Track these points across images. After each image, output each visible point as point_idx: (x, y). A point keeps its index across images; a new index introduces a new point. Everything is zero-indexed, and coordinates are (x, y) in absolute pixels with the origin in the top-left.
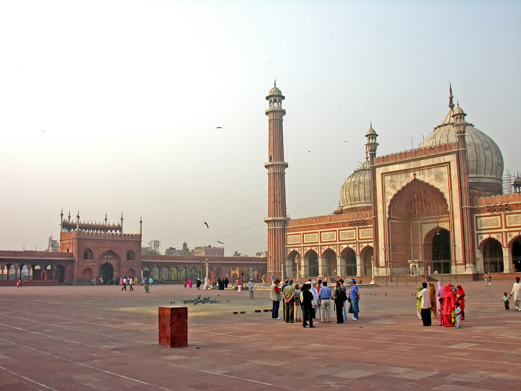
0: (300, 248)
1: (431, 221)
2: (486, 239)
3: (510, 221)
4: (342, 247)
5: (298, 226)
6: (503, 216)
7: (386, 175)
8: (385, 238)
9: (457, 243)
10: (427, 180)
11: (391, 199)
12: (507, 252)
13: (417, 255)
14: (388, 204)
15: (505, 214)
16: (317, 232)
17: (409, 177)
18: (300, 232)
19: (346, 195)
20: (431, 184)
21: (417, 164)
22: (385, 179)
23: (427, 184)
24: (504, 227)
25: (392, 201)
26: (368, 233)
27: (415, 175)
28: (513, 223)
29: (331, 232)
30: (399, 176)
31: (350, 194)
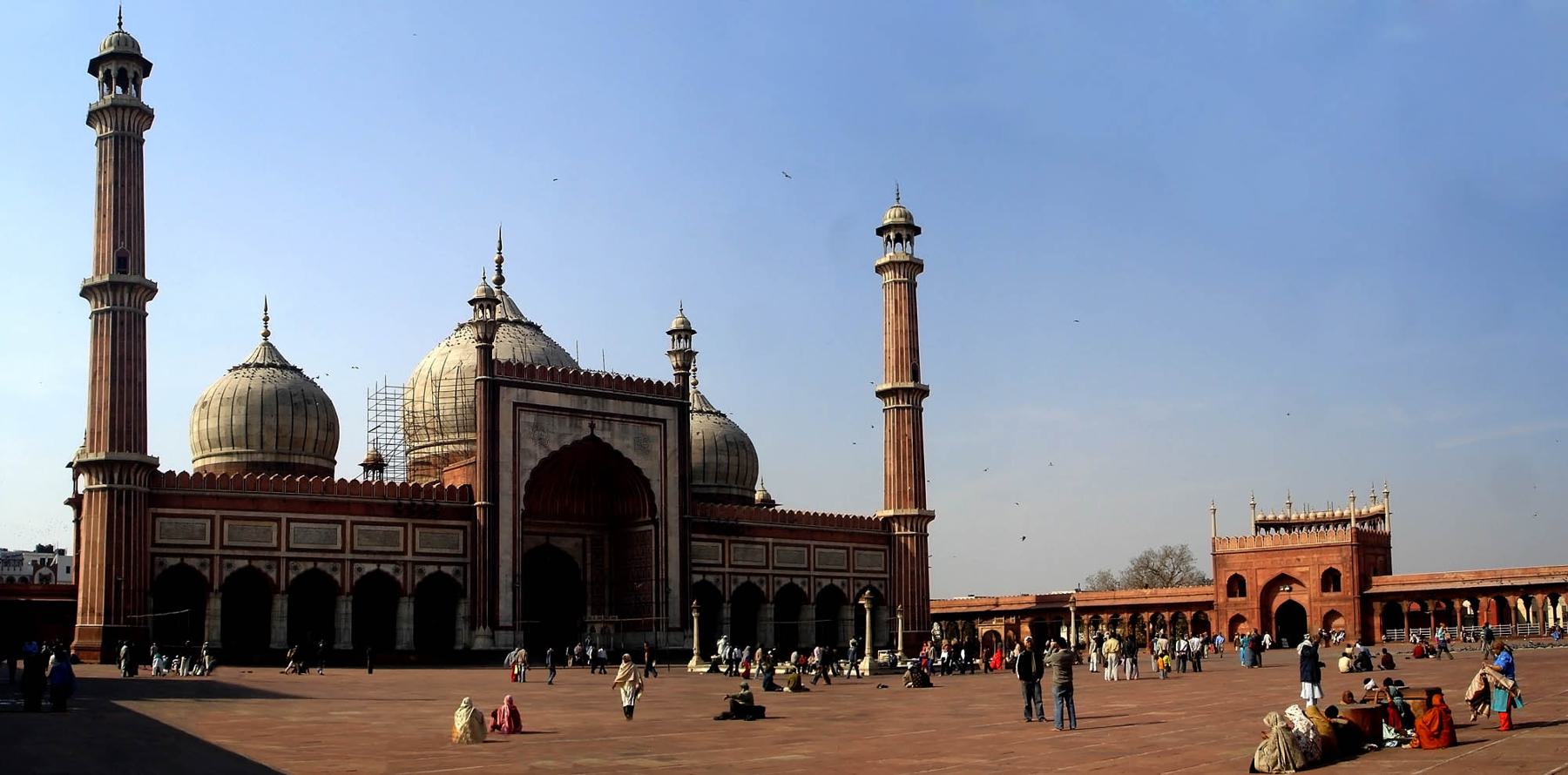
0: (208, 560)
1: (533, 530)
4: (360, 570)
5: (208, 494)
6: (727, 543)
9: (671, 586)
10: (617, 445)
12: (729, 612)
14: (525, 478)
15: (731, 542)
16: (278, 520)
18: (212, 512)
20: (626, 456)
23: (618, 454)
24: (727, 565)
25: (535, 472)
27: (592, 426)
29: (325, 526)
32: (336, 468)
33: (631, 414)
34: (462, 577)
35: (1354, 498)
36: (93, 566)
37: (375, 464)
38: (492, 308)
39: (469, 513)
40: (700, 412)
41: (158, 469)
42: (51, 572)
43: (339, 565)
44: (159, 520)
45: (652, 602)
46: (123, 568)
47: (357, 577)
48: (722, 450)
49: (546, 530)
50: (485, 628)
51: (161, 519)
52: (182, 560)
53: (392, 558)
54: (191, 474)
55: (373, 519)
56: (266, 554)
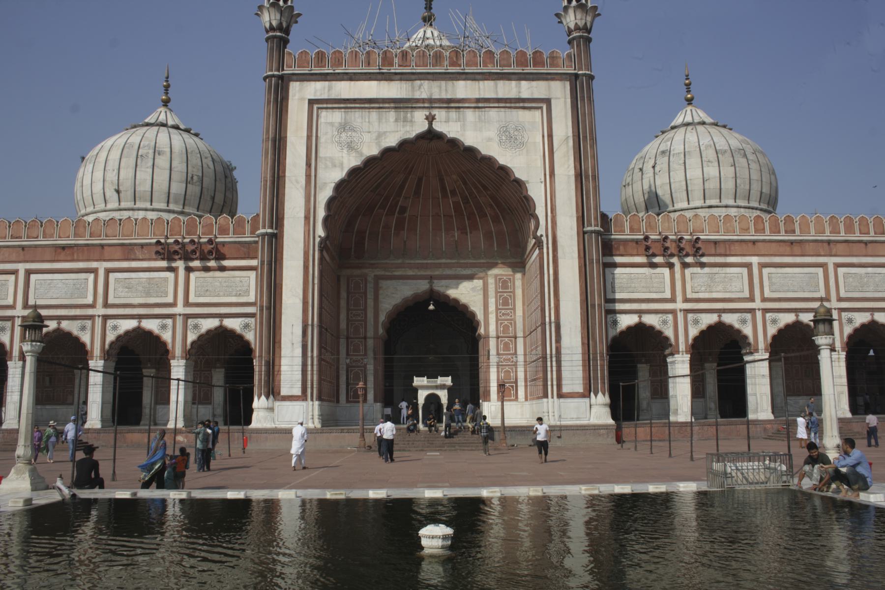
1: (410, 273)
2: (630, 329)
3: (696, 285)
4: (115, 328)
6: (678, 267)
7: (325, 106)
8: (307, 303)
10: (469, 139)
13: (358, 367)
14: (325, 194)
15: (685, 265)
17: (408, 124)
19: (104, 181)
21: (440, 90)
22: (322, 120)
23: (471, 152)
24: (679, 298)
25: (340, 186)
26: (224, 285)
27: (431, 119)
28: (703, 289)
30: (374, 114)
31: (120, 178)
34: (252, 333)
43: (89, 323)
47: (111, 337)
48: (709, 161)
49: (429, 273)
50: (259, 398)
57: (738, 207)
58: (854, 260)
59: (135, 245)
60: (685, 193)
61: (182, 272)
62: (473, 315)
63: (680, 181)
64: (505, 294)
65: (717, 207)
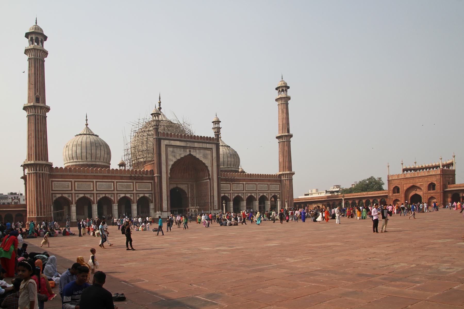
0: (71, 195)
2: (223, 196)
4: (119, 196)
5: (69, 174)
9: (215, 197)
10: (198, 156)
11: (172, 164)
14: (170, 167)
15: (232, 184)
16: (93, 182)
18: (71, 180)
20: (200, 159)
22: (168, 150)
23: (198, 159)
25: (173, 165)
27: (190, 151)
29: (108, 183)
30: (179, 149)
32: (111, 166)
33: (201, 147)
34: (151, 197)
35: (442, 158)
36: (32, 198)
37: (122, 165)
38: (158, 116)
39: (153, 178)
40: (222, 146)
41: (52, 166)
42: (18, 201)
43: (113, 195)
44: (53, 183)
45: (209, 202)
46: (42, 198)
47: (119, 198)
51: (54, 182)
52: (62, 195)
53: (129, 192)
54: (64, 168)
55: (123, 181)
56: (89, 192)
57: (234, 168)
58: (261, 183)
59: (124, 176)
60: (223, 164)
61: (135, 183)
62: (185, 192)
63: (222, 161)
64: (192, 188)
65: (230, 168)
